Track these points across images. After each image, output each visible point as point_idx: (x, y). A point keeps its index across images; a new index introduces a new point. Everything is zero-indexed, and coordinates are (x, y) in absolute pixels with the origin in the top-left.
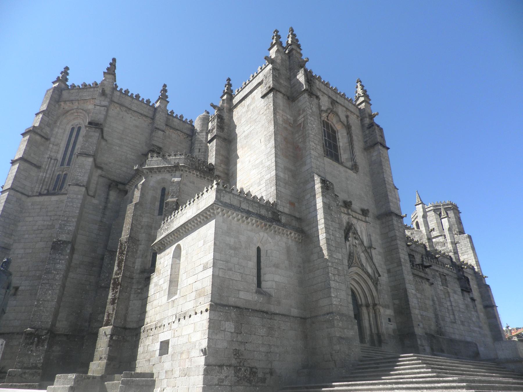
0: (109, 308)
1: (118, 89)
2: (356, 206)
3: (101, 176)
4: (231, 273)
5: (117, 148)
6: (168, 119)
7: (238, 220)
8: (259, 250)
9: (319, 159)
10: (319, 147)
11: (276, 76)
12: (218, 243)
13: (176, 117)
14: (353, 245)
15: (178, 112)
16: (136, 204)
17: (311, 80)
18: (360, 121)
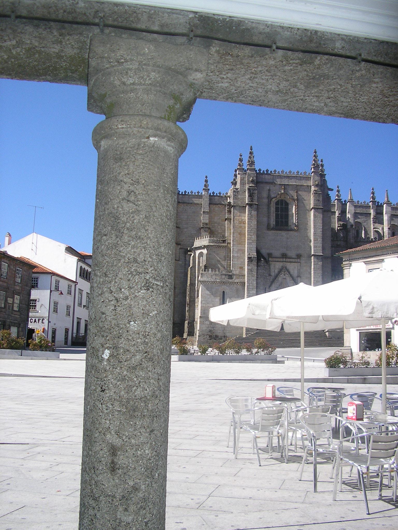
0: (187, 313)
1: (180, 193)
2: (292, 253)
3: (180, 248)
4: (208, 305)
5: (186, 230)
6: (210, 200)
7: (211, 283)
8: (224, 292)
9: (253, 244)
10: (253, 237)
11: (235, 195)
12: (202, 295)
13: (217, 196)
14: (283, 278)
15: (217, 192)
16: (191, 268)
17: (253, 193)
18: (310, 188)
